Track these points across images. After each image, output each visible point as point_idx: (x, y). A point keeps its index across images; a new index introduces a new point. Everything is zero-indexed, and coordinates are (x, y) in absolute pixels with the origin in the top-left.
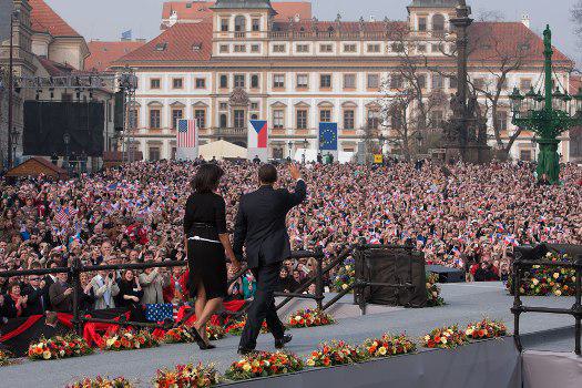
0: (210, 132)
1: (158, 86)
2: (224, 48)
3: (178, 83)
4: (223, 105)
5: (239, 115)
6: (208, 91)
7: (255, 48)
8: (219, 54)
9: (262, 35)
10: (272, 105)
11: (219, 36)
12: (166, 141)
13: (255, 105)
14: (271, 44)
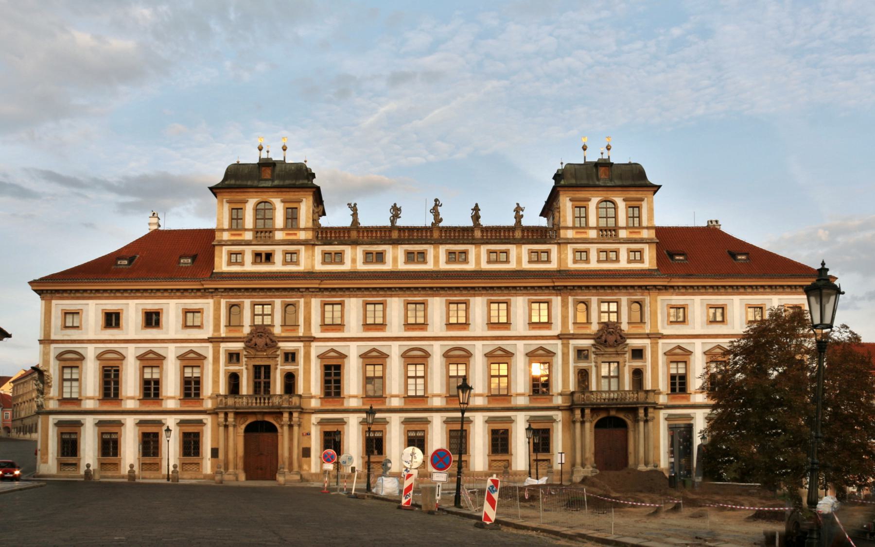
0: (209, 405)
1: (118, 325)
2: (235, 257)
3: (152, 319)
4: (233, 357)
5: (262, 375)
6: (208, 332)
9: (302, 235)
10: (321, 357)
11: (226, 236)
12: (130, 422)
13: (291, 357)
14: (319, 250)
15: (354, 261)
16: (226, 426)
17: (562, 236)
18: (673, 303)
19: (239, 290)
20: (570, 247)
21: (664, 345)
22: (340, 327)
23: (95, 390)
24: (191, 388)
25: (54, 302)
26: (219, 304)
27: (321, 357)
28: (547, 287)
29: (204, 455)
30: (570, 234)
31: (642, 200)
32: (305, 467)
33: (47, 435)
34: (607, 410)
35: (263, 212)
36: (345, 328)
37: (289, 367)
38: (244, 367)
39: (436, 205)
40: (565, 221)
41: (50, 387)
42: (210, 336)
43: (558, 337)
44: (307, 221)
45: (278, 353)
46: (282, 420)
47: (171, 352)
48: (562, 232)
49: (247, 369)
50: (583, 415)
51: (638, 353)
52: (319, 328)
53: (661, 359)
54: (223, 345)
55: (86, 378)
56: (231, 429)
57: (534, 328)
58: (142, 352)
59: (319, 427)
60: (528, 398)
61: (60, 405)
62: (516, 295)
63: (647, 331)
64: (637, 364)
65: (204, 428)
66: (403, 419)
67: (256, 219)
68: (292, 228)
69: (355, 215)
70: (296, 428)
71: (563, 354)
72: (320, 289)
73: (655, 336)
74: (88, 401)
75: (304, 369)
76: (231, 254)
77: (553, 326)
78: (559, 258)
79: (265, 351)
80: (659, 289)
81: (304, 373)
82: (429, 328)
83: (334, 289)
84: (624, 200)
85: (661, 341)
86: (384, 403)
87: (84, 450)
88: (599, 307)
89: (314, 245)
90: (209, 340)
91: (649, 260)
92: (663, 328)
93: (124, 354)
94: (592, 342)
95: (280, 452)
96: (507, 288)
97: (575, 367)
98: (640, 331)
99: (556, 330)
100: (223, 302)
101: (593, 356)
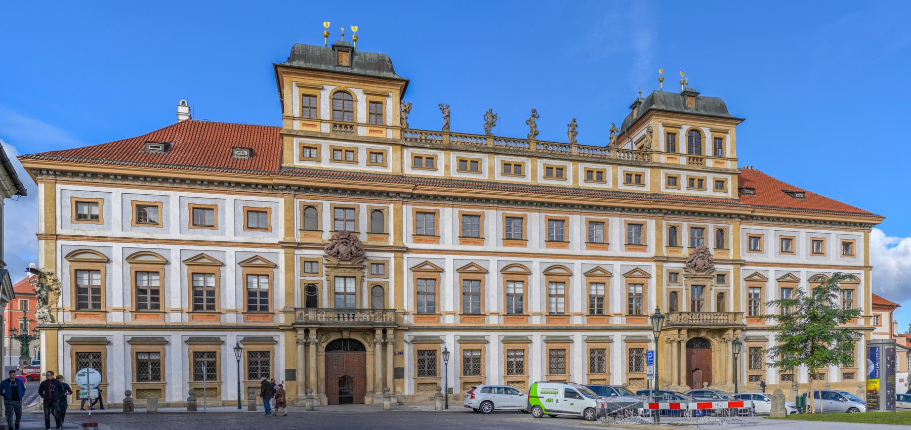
6: (279, 234)
7: (376, 156)
9: (390, 134)
14: (408, 153)
24: (257, 302)
37: (376, 280)
44: (394, 119)
45: (365, 263)
49: (327, 280)
52: (411, 238)
55: (111, 285)
68: (376, 125)
79: (350, 260)
80: (742, 219)
83: (427, 197)
89: (403, 146)
90: (284, 245)
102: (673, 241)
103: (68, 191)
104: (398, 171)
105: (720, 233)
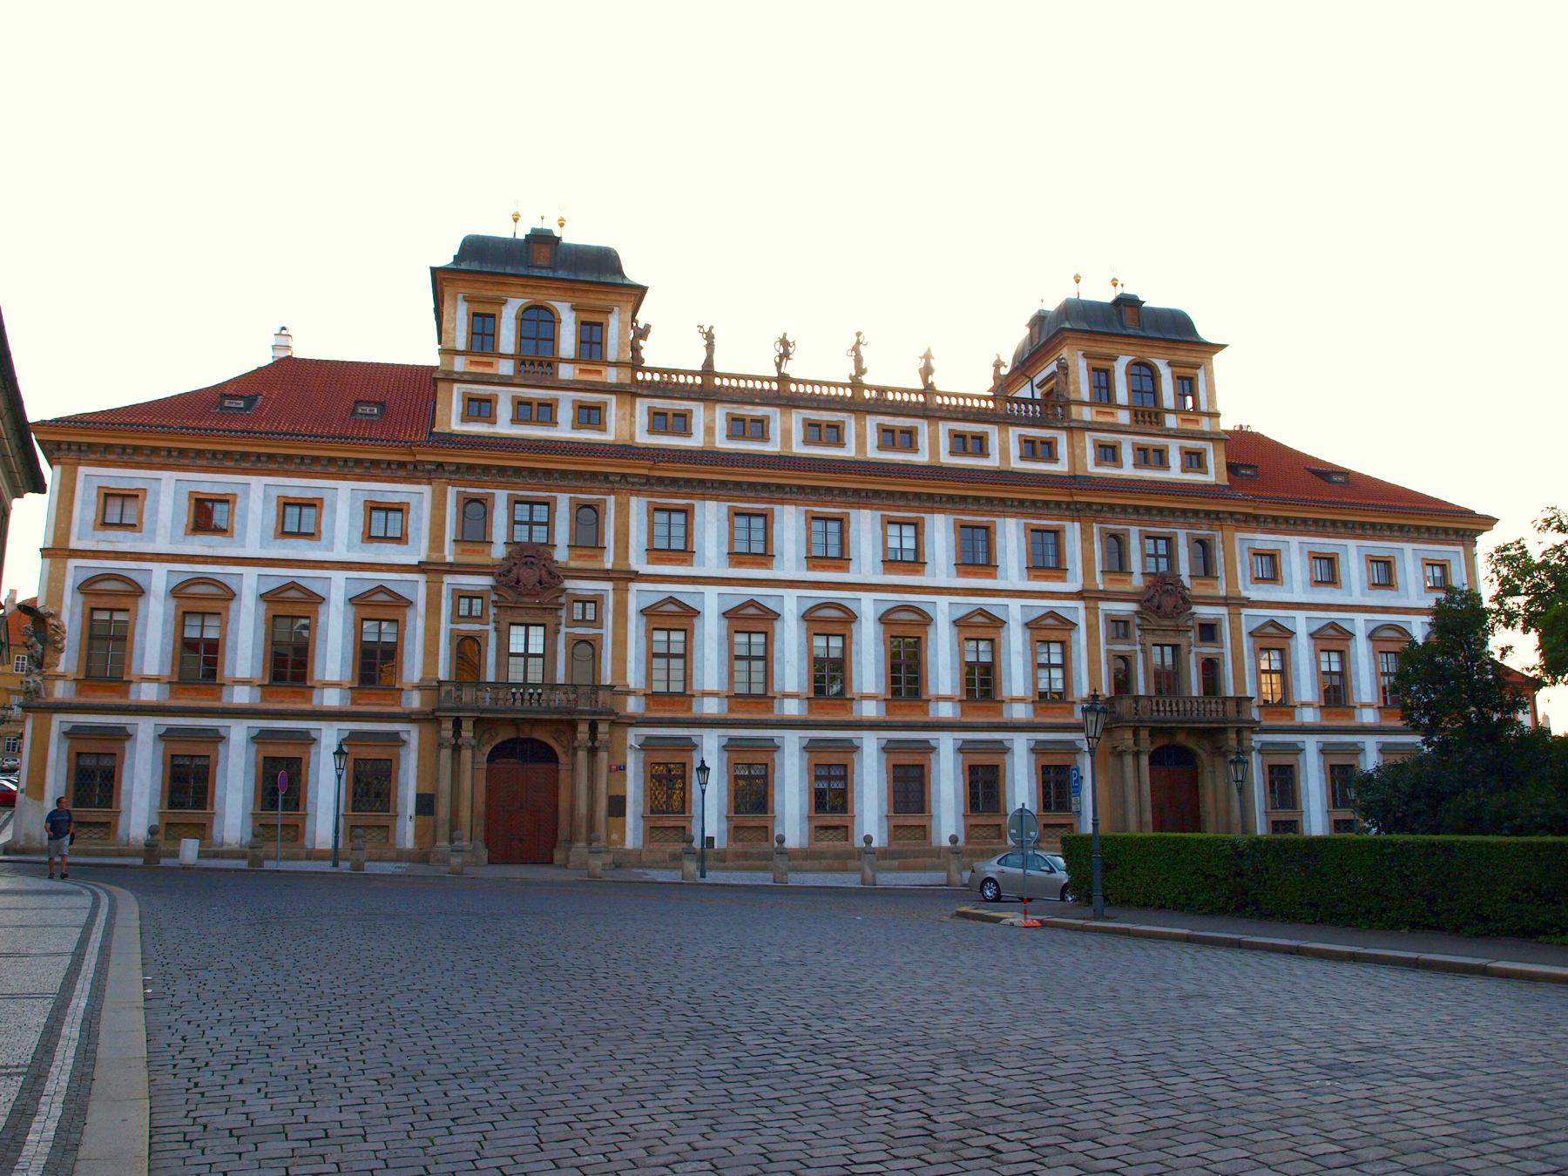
0: (414, 701)
2: (480, 408)
3: (297, 518)
7: (590, 415)
8: (457, 426)
9: (611, 376)
10: (648, 613)
11: (460, 364)
12: (238, 733)
14: (642, 406)
15: (709, 430)
16: (456, 749)
17: (1074, 416)
18: (1258, 545)
19: (486, 469)
20: (1089, 439)
21: (1251, 618)
22: (686, 554)
23: (162, 663)
24: (374, 664)
25: (83, 471)
26: (445, 495)
27: (648, 613)
28: (1058, 504)
29: (400, 809)
30: (1087, 414)
31: (1197, 367)
32: (614, 837)
33: (44, 758)
34: (1170, 732)
35: (538, 323)
36: (696, 557)
38: (491, 627)
39: (859, 343)
40: (1078, 391)
41: (61, 651)
42: (423, 558)
43: (1079, 596)
44: (621, 349)
45: (562, 600)
46: (574, 737)
47: (338, 588)
48: (1074, 409)
49: (496, 629)
50: (1136, 743)
51: (1209, 631)
52: (644, 556)
53: (1247, 643)
54: (448, 579)
55: (144, 635)
56: (467, 754)
57: (1036, 577)
58: (273, 584)
59: (642, 755)
60: (1031, 707)
61: (79, 692)
62: (1004, 515)
63: (1223, 593)
64: (1209, 650)
65: (402, 751)
66: (805, 743)
67: (522, 337)
69: (710, 347)
70: (603, 756)
71: (1089, 627)
72: (648, 478)
73: (1235, 603)
74: (144, 685)
75: (614, 634)
76: (470, 400)
77: (1069, 575)
78: (1073, 456)
79: (536, 595)
80: (1237, 521)
81: (614, 644)
82: (853, 566)
83: (674, 481)
84: (1170, 364)
85: (1245, 611)
86: (770, 708)
87: (130, 793)
88: (1142, 544)
89: (634, 395)
90: (420, 568)
91: (1213, 473)
92: (1246, 588)
93: (233, 587)
94: (1130, 607)
95: (563, 804)
96: (989, 500)
97: (1108, 651)
98: (1209, 592)
99: (1074, 584)
100: (452, 492)
101: (1138, 633)
102: (1118, 563)
103: (92, 477)
104: (624, 439)
105: (1203, 548)
